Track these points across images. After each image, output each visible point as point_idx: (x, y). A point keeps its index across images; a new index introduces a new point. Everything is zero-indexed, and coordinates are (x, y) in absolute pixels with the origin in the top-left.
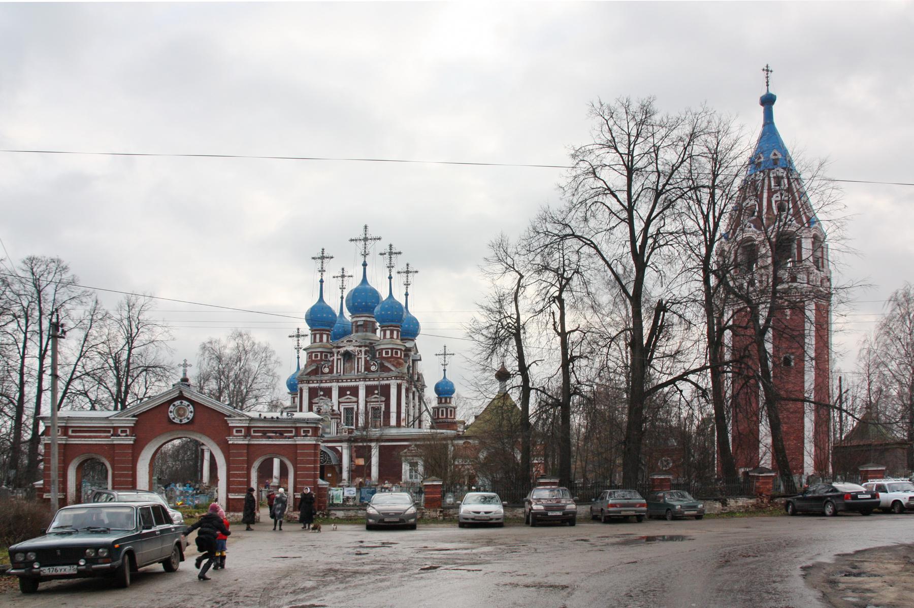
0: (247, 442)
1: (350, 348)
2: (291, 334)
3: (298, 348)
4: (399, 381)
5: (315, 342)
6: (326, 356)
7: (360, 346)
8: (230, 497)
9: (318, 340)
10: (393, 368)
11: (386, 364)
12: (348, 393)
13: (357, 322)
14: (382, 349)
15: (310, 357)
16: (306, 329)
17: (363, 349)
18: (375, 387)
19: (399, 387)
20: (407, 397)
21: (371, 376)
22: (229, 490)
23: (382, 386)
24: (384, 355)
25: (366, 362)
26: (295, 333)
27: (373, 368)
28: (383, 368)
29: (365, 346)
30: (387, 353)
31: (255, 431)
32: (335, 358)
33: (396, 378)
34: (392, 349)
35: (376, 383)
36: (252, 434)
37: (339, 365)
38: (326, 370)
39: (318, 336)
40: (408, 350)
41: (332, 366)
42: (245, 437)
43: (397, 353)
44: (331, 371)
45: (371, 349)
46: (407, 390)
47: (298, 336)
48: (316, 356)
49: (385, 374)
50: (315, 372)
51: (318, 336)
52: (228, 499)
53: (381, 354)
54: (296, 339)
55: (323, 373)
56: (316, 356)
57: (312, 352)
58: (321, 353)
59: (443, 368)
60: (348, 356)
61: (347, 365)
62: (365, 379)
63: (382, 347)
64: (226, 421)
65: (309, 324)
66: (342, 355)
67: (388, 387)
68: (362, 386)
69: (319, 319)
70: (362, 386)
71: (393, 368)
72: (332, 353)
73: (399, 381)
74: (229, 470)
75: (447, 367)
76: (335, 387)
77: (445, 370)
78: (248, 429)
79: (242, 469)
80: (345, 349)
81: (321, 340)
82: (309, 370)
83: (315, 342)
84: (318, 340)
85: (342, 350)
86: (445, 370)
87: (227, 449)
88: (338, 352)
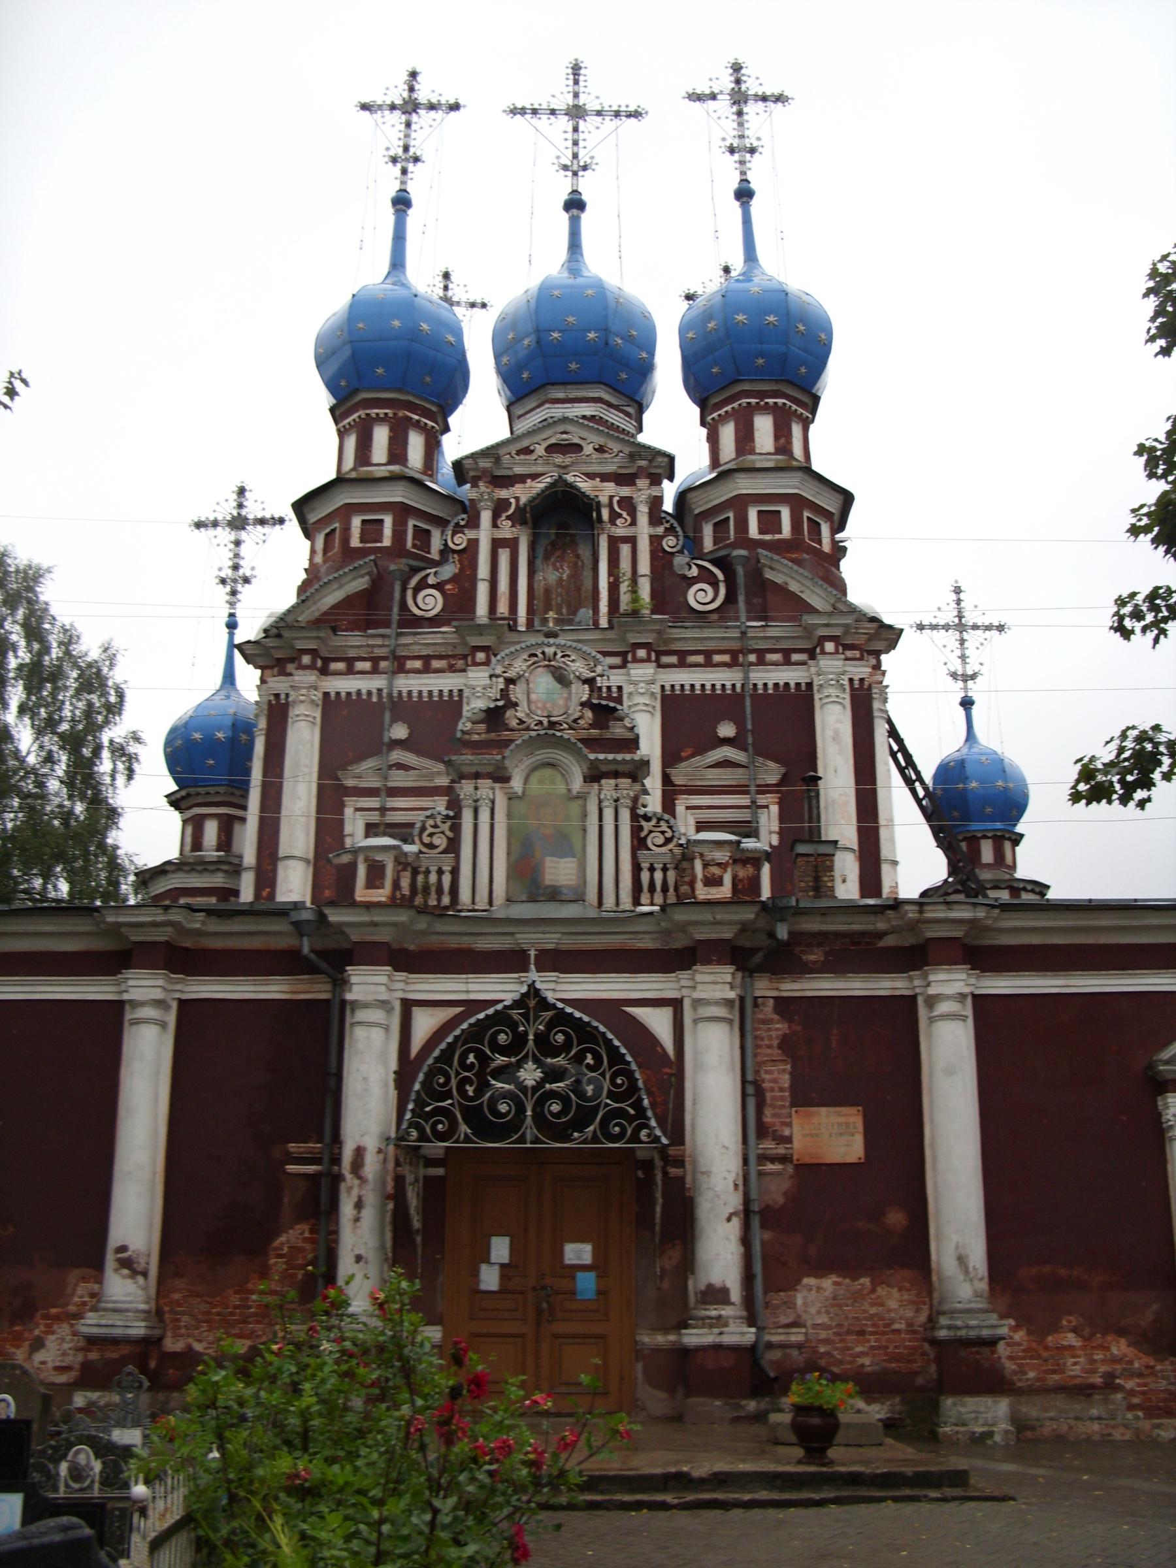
2: (207, 515)
6: (423, 536)
11: (780, 573)
14: (741, 503)
18: (725, 703)
21: (688, 636)
24: (753, 531)
25: (661, 559)
26: (227, 510)
27: (700, 597)
30: (769, 521)
32: (484, 535)
34: (797, 503)
35: (722, 678)
37: (504, 573)
38: (431, 602)
39: (381, 436)
41: (465, 582)
44: (460, 601)
47: (238, 523)
48: (372, 529)
49: (777, 630)
51: (381, 436)
54: (225, 535)
56: (372, 529)
57: (350, 509)
58: (402, 511)
59: (956, 691)
62: (658, 654)
63: (745, 485)
65: (332, 386)
66: (519, 518)
67: (799, 706)
75: (976, 690)
77: (967, 704)
81: (397, 453)
85: (523, 493)
86: (967, 704)
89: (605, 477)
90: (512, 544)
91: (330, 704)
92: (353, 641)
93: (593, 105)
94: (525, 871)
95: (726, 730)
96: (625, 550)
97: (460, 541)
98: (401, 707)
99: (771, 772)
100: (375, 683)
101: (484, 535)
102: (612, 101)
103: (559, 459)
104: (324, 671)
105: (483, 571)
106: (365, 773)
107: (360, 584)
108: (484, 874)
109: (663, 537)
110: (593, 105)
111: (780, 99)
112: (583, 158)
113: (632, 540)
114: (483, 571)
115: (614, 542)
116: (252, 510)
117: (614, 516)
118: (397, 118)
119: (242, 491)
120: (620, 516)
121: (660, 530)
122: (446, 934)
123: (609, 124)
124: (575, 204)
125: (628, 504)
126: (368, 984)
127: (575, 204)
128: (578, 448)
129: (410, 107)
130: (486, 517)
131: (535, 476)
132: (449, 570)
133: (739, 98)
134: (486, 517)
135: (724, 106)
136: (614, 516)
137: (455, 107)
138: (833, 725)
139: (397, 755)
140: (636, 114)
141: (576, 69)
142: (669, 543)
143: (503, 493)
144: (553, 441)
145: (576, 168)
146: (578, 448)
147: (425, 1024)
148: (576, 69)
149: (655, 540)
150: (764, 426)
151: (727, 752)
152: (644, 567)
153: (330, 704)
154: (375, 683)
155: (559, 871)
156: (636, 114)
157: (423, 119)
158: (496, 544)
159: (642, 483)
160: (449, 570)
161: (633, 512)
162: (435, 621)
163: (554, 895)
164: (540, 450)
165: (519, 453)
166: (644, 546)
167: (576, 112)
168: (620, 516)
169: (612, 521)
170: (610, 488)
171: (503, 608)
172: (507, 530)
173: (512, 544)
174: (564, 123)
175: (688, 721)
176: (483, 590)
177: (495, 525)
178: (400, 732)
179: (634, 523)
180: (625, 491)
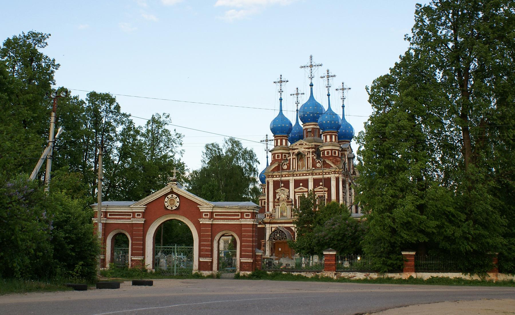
0: (211, 223)
1: (302, 150)
3: (267, 150)
4: (337, 175)
5: (277, 145)
6: (285, 156)
7: (308, 148)
8: (201, 260)
9: (279, 144)
10: (332, 165)
11: (328, 162)
12: (301, 184)
14: (324, 150)
15: (274, 157)
16: (271, 136)
17: (311, 150)
18: (320, 180)
19: (337, 179)
20: (344, 187)
22: (200, 256)
23: (325, 179)
25: (313, 160)
26: (265, 139)
27: (318, 165)
28: (325, 165)
29: (312, 148)
31: (216, 215)
32: (291, 157)
33: (335, 172)
34: (332, 150)
35: (321, 177)
36: (215, 217)
37: (294, 163)
38: (285, 167)
39: (279, 141)
40: (343, 150)
41: (290, 163)
42: (210, 219)
43: (335, 153)
44: (289, 168)
45: (317, 152)
46: (344, 182)
47: (267, 141)
49: (327, 170)
50: (277, 169)
51: (279, 141)
52: (199, 262)
53: (324, 154)
55: (283, 169)
56: (278, 156)
60: (300, 156)
61: (300, 163)
63: (325, 148)
64: (198, 208)
67: (329, 179)
68: (311, 178)
69: (281, 129)
70: (311, 178)
71: (332, 165)
73: (337, 175)
74: (200, 241)
76: (292, 179)
78: (212, 213)
79: (208, 241)
81: (281, 144)
82: (273, 167)
83: (277, 145)
84: (279, 144)
85: (296, 151)
87: (199, 226)
89: (306, 148)
91: (274, 181)
92: (276, 173)
93: (314, 65)
94: (281, 213)
95: (321, 184)
97: (288, 158)
98: (282, 182)
99: (326, 189)
100: (279, 179)
101: (291, 157)
102: (317, 63)
104: (273, 177)
105: (291, 163)
106: (278, 191)
107: (277, 165)
108: (278, 215)
110: (314, 65)
111: (334, 76)
112: (313, 76)
114: (291, 163)
115: (307, 158)
116: (269, 139)
118: (279, 84)
119: (267, 135)
122: (275, 221)
123: (316, 68)
124: (311, 85)
126: (267, 226)
127: (311, 85)
129: (281, 82)
132: (288, 162)
133: (328, 77)
135: (326, 78)
137: (287, 81)
138: (333, 183)
139: (282, 188)
140: (321, 65)
141: (311, 57)
142: (315, 157)
145: (311, 78)
147: (273, 229)
148: (311, 57)
150: (328, 137)
151: (321, 187)
152: (311, 162)
153: (274, 181)
154: (279, 179)
155: (285, 214)
156: (321, 65)
157: (283, 84)
158: (293, 158)
160: (288, 162)
162: (287, 169)
163: (284, 216)
167: (311, 66)
170: (307, 150)
172: (294, 157)
173: (295, 158)
174: (309, 68)
175: (316, 182)
178: (282, 185)
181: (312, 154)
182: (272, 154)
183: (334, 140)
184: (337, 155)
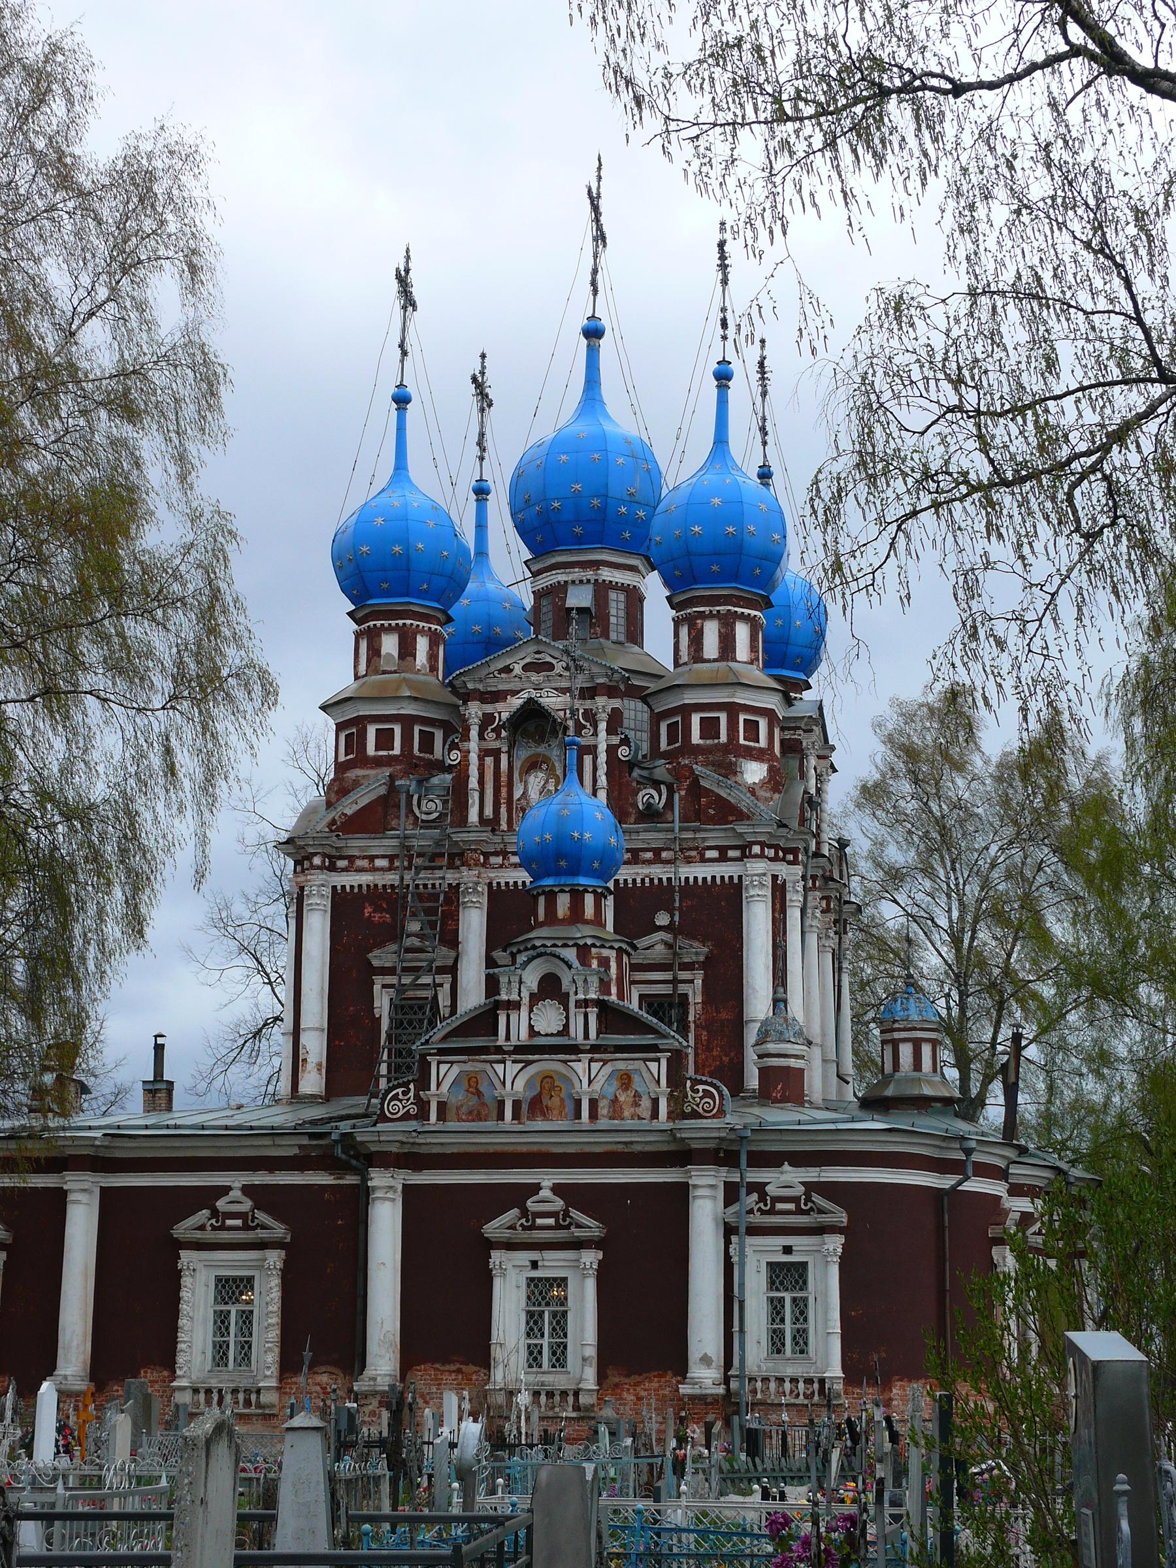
13: (561, 589)
14: (686, 711)
23: (691, 889)
24: (696, 738)
30: (710, 728)
32: (473, 745)
34: (733, 710)
38: (432, 807)
39: (390, 644)
53: (678, 732)
56: (384, 739)
57: (360, 722)
58: (407, 722)
63: (690, 698)
72: (455, 730)
80: (516, 702)
88: (487, 719)
90: (496, 754)
96: (588, 759)
103: (534, 677)
105: (473, 783)
109: (619, 746)
113: (592, 750)
117: (579, 728)
120: (585, 727)
121: (615, 740)
125: (591, 716)
128: (551, 667)
130: (474, 733)
131: (514, 693)
134: (474, 733)
136: (579, 728)
143: (489, 708)
144: (528, 660)
146: (551, 667)
149: (611, 750)
150: (711, 633)
158: (484, 753)
159: (601, 701)
161: (595, 726)
164: (518, 669)
165: (501, 671)
166: (602, 757)
168: (585, 727)
169: (578, 733)
171: (489, 812)
173: (496, 754)
176: (474, 799)
177: (481, 737)
179: (595, 734)
180: (588, 704)
181: (610, 731)
182: (340, 727)
183: (742, 650)
184: (763, 743)
